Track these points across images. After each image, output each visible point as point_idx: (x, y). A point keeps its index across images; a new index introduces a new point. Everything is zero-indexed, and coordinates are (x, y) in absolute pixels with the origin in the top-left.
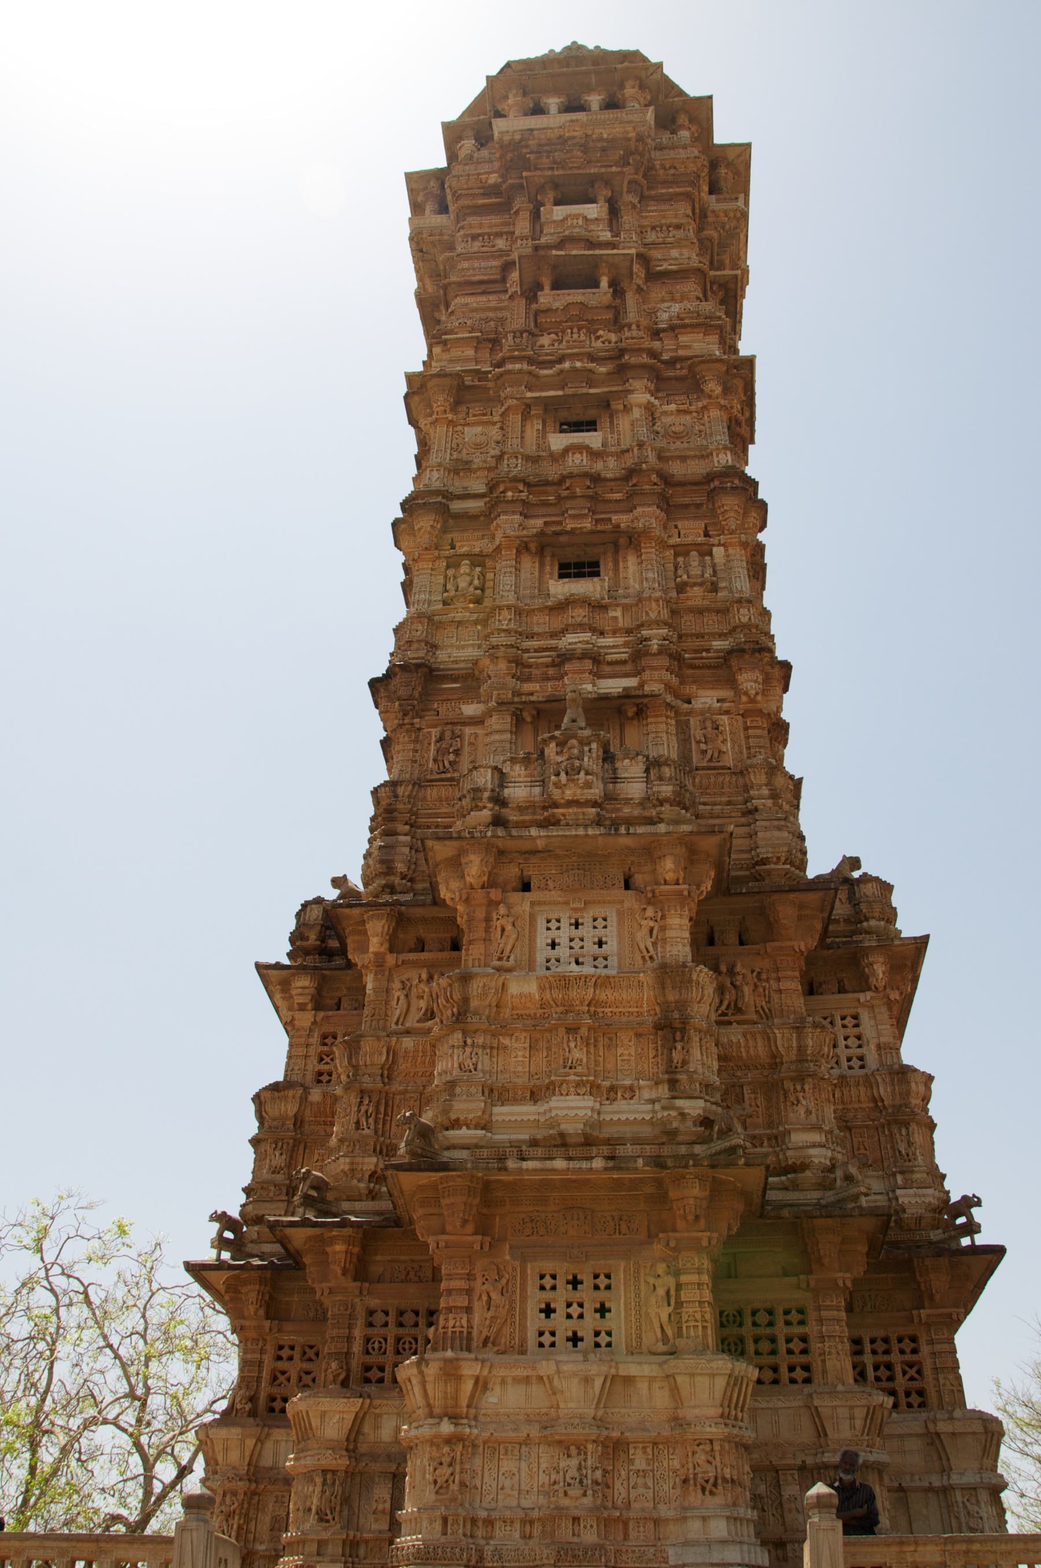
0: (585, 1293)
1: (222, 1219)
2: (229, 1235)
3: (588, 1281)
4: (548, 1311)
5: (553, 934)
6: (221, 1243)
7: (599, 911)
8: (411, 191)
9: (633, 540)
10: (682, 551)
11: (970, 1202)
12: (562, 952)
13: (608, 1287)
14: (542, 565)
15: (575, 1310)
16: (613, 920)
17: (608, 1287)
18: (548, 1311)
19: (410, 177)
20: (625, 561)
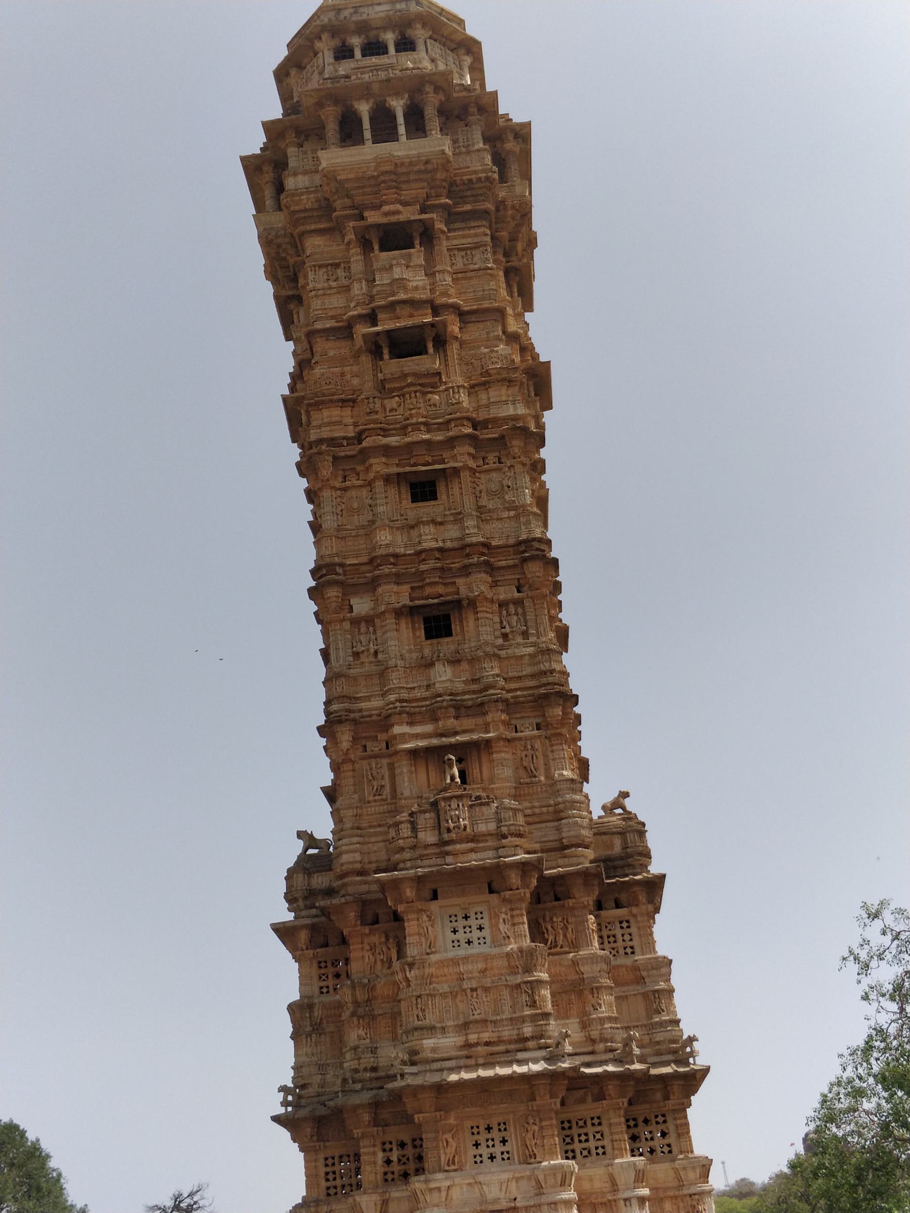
0: (495, 1134)
1: (283, 1089)
2: (290, 1098)
3: (496, 1128)
5: (454, 924)
6: (285, 1103)
8: (245, 168)
10: (503, 605)
11: (692, 1040)
12: (460, 935)
13: (505, 1130)
14: (413, 623)
15: (490, 1143)
16: (486, 915)
17: (505, 1130)
19: (243, 159)
20: (467, 618)
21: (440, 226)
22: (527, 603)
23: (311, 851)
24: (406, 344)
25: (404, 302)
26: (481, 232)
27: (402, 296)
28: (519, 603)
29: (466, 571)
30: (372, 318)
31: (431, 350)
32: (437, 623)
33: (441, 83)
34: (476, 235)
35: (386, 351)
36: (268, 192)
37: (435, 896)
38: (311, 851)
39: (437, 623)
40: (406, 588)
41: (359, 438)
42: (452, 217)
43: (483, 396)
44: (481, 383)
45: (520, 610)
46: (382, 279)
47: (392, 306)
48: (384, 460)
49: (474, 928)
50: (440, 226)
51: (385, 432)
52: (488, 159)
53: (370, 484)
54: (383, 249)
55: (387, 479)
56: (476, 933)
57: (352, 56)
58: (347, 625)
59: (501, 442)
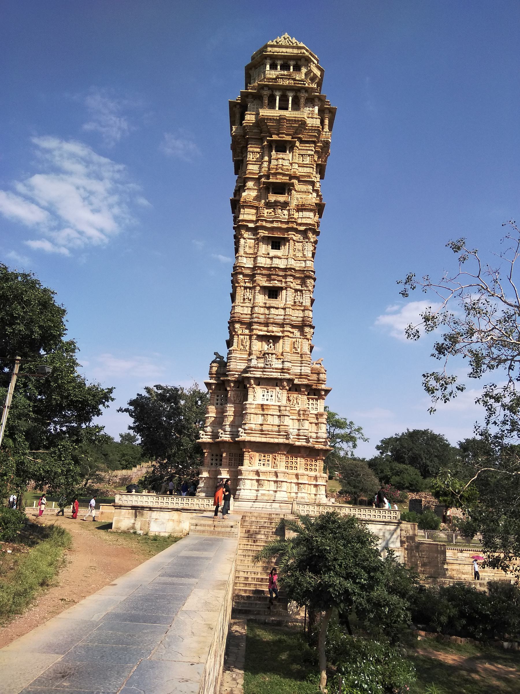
4: (260, 460)
7: (272, 390)
10: (296, 291)
18: (260, 460)
21: (297, 144)
23: (218, 359)
26: (310, 149)
27: (280, 171)
28: (301, 291)
32: (273, 293)
34: (309, 150)
35: (271, 190)
36: (238, 116)
37: (259, 385)
38: (218, 359)
39: (273, 293)
43: (301, 213)
44: (301, 208)
46: (274, 162)
47: (276, 174)
49: (270, 395)
50: (297, 144)
52: (319, 120)
56: (270, 397)
57: (276, 69)
58: (243, 288)
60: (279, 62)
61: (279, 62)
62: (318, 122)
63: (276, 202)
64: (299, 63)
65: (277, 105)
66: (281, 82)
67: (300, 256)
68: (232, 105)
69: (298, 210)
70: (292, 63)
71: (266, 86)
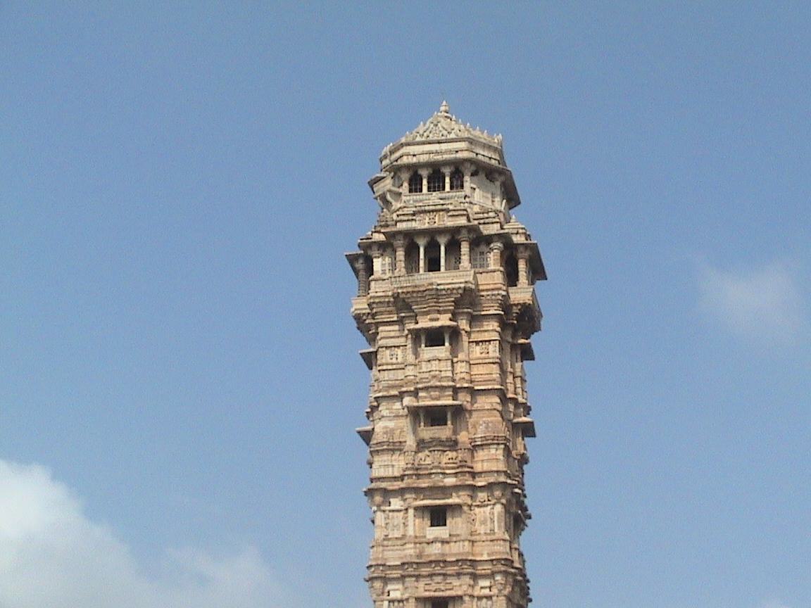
9: (461, 597)
10: (480, 598)
22: (494, 598)
24: (435, 416)
25: (436, 387)
28: (489, 598)
29: (458, 575)
30: (415, 394)
31: (449, 422)
33: (472, 229)
35: (422, 420)
40: (421, 584)
41: (402, 478)
42: (474, 319)
45: (489, 603)
46: (425, 367)
47: (426, 389)
48: (414, 496)
51: (418, 476)
53: (407, 509)
54: (426, 346)
55: (416, 509)
58: (386, 603)
59: (489, 487)
60: (424, 173)
61: (424, 173)
62: (498, 278)
63: (433, 440)
64: (462, 168)
65: (422, 263)
66: (422, 223)
67: (482, 532)
68: (352, 259)
69: (474, 448)
70: (447, 171)
71: (400, 232)
